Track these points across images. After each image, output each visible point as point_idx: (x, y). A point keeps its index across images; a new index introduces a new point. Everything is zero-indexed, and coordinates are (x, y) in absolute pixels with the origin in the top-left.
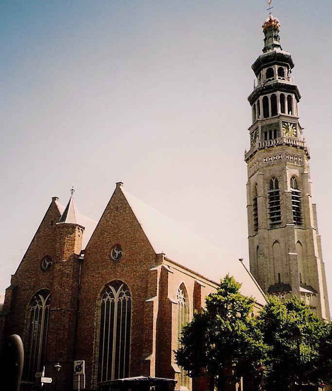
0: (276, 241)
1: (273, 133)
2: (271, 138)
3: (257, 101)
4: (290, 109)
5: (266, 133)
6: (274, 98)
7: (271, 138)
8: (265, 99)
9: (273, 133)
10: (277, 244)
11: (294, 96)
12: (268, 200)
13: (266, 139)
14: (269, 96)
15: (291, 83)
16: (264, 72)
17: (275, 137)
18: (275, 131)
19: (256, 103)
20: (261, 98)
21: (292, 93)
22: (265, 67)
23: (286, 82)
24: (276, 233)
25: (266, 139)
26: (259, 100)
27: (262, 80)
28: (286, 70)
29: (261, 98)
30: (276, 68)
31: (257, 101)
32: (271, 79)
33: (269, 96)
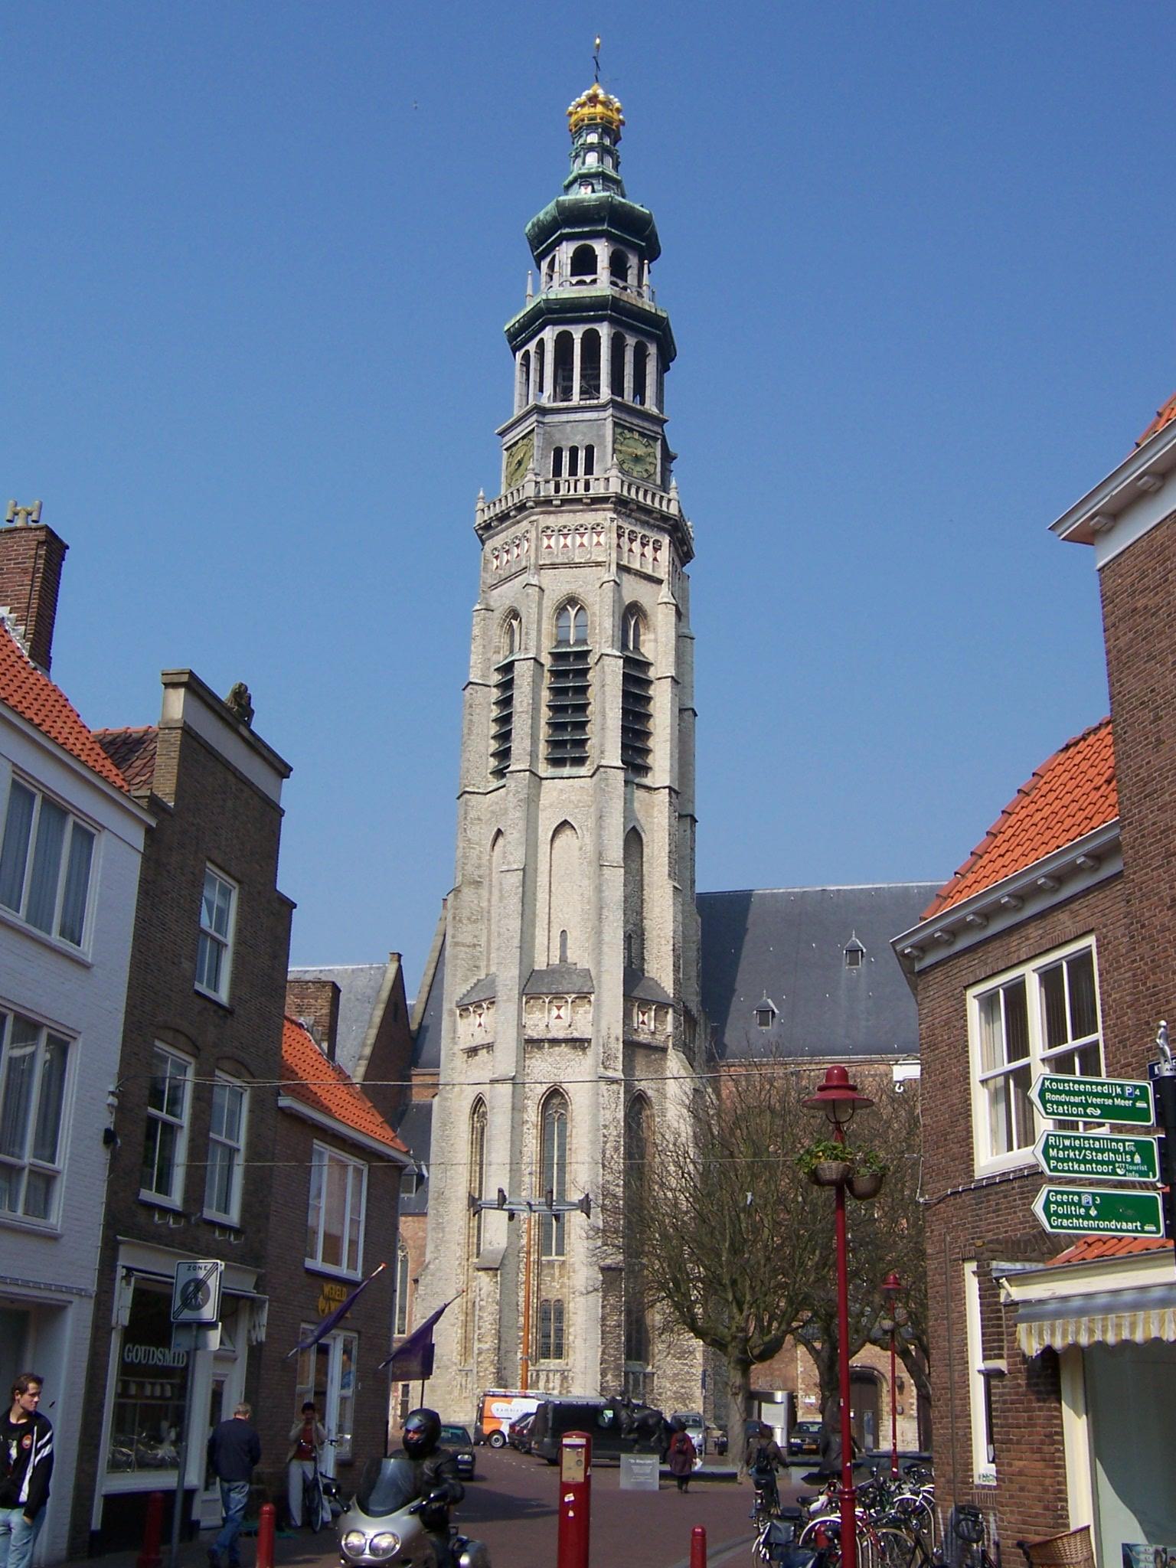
0: (565, 823)
1: (582, 455)
2: (573, 472)
3: (549, 259)
4: (640, 389)
5: (558, 452)
6: (591, 341)
7: (573, 472)
8: (564, 343)
9: (582, 455)
10: (567, 835)
11: (652, 349)
12: (547, 680)
13: (557, 472)
15: (647, 304)
16: (566, 252)
17: (589, 470)
18: (590, 450)
19: (532, 347)
20: (549, 334)
22: (570, 237)
23: (630, 296)
24: (564, 793)
25: (557, 472)
26: (542, 340)
27: (555, 276)
28: (633, 261)
29: (549, 334)
30: (602, 250)
31: (549, 259)
32: (588, 279)
33: (577, 333)
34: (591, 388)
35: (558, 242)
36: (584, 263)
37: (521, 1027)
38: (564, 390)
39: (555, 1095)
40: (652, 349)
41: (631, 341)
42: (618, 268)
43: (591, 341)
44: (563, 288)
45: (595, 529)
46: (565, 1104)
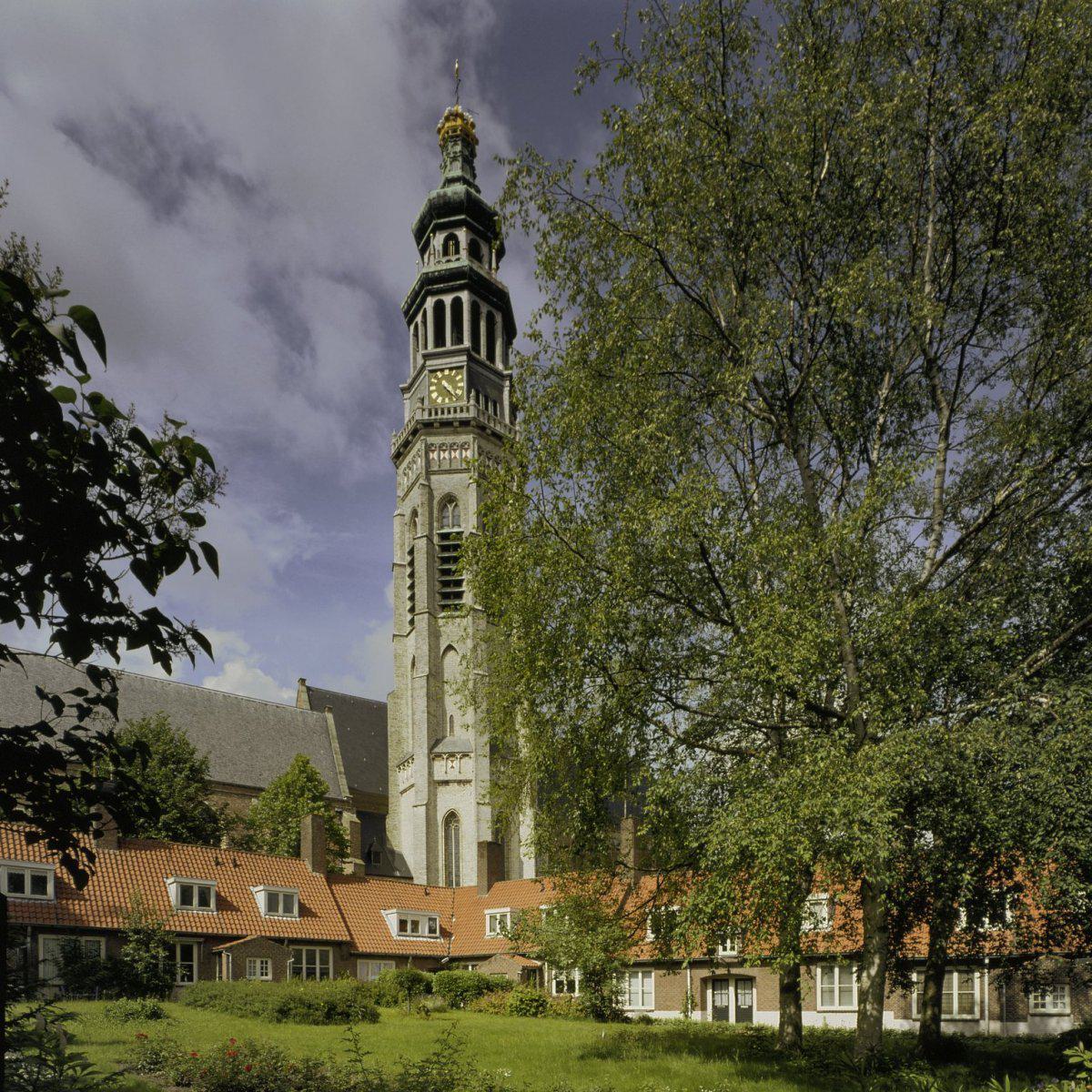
8: (439, 307)
11: (499, 318)
14: (448, 299)
16: (438, 240)
20: (430, 303)
21: (498, 308)
29: (430, 303)
33: (448, 299)
34: (458, 339)
35: (434, 231)
36: (450, 245)
37: (430, 774)
38: (440, 340)
39: (452, 817)
40: (499, 318)
41: (484, 309)
42: (474, 252)
43: (457, 303)
44: (436, 265)
45: (463, 447)
46: (458, 821)
